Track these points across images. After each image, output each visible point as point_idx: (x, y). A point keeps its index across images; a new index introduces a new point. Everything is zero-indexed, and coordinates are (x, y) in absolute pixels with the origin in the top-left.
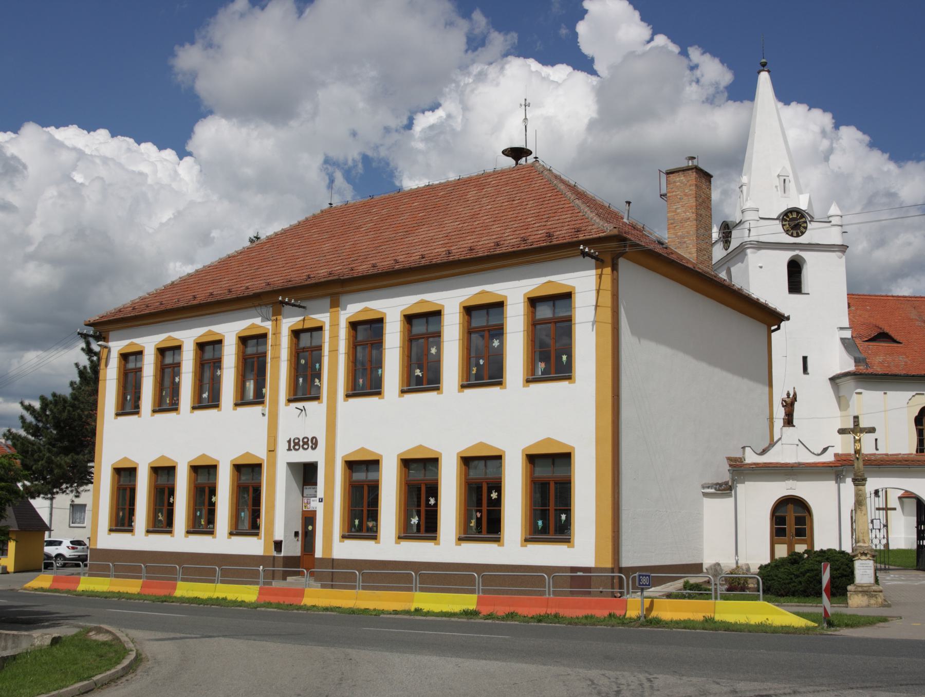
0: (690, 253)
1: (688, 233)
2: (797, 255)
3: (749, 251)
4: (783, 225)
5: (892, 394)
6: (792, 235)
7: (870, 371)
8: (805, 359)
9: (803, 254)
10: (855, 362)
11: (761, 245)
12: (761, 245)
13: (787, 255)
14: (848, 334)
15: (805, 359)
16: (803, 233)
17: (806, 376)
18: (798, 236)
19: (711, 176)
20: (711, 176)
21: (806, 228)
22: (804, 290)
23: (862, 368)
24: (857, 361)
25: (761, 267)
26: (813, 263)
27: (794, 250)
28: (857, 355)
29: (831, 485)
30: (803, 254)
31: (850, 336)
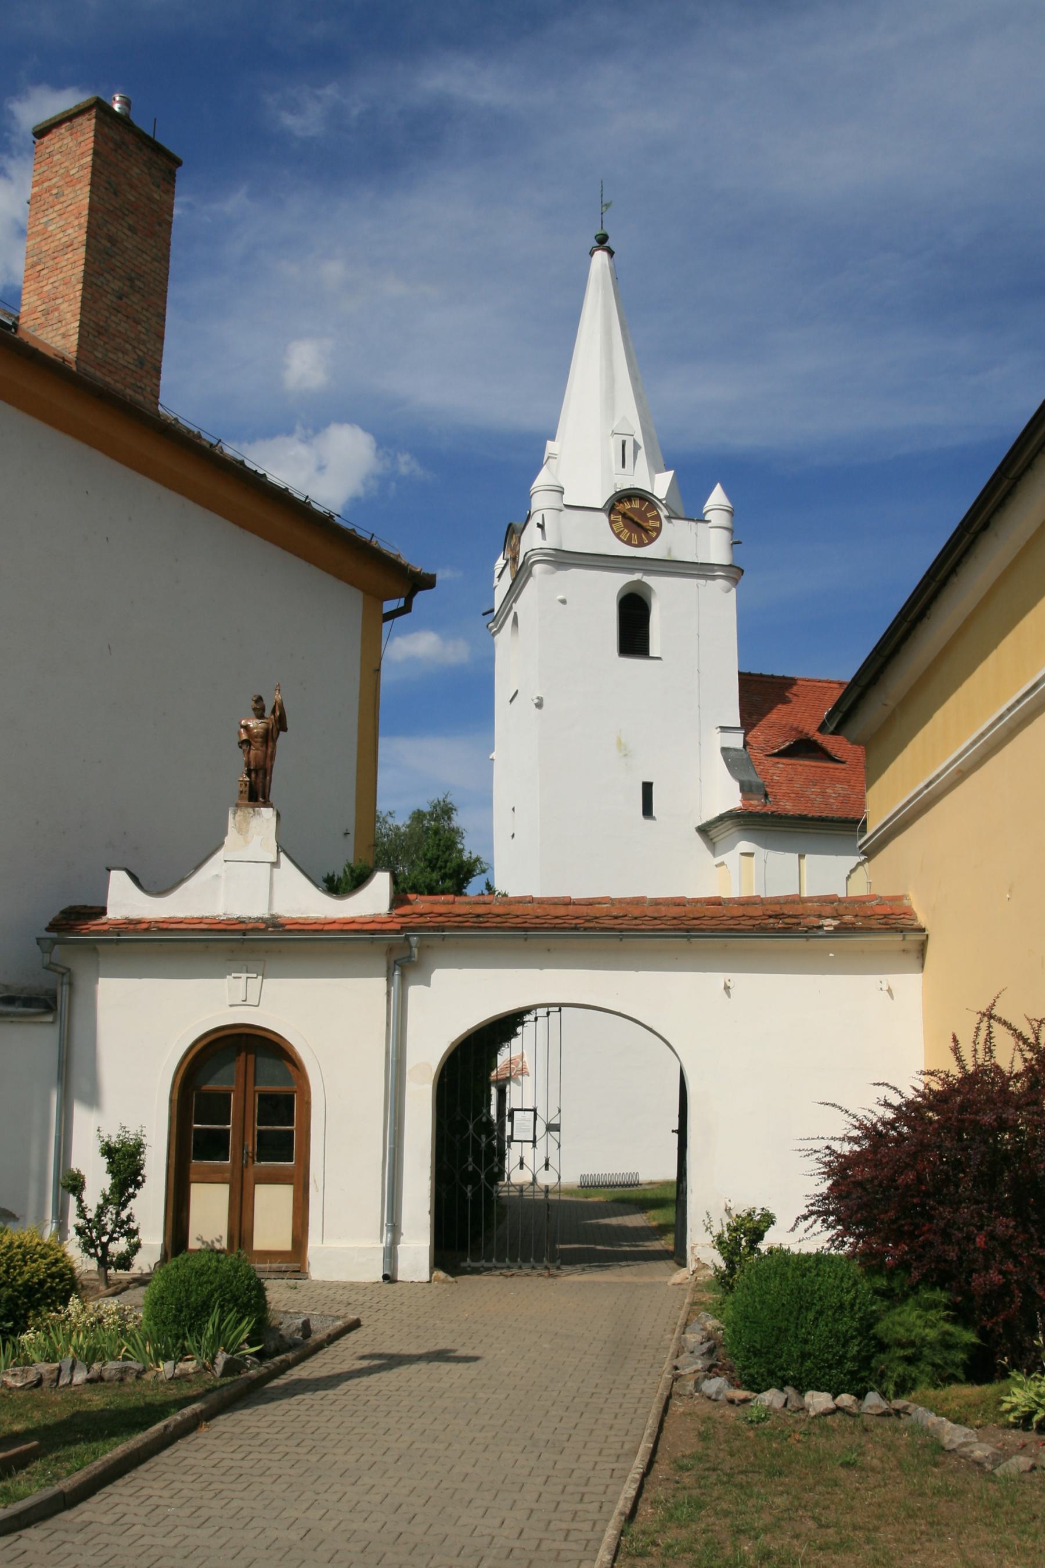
0: (64, 336)
1: (66, 283)
2: (639, 582)
3: (537, 569)
4: (611, 523)
5: (811, 860)
6: (628, 542)
7: (770, 808)
8: (647, 788)
9: (651, 580)
10: (742, 790)
11: (563, 559)
12: (563, 559)
13: (617, 582)
14: (736, 740)
15: (647, 788)
16: (652, 540)
17: (649, 822)
18: (641, 544)
19: (178, 163)
20: (178, 163)
21: (658, 530)
22: (654, 649)
23: (756, 804)
24: (746, 789)
25: (564, 602)
26: (667, 598)
27: (631, 571)
28: (745, 778)
29: (369, 991)
30: (652, 581)
31: (740, 745)
